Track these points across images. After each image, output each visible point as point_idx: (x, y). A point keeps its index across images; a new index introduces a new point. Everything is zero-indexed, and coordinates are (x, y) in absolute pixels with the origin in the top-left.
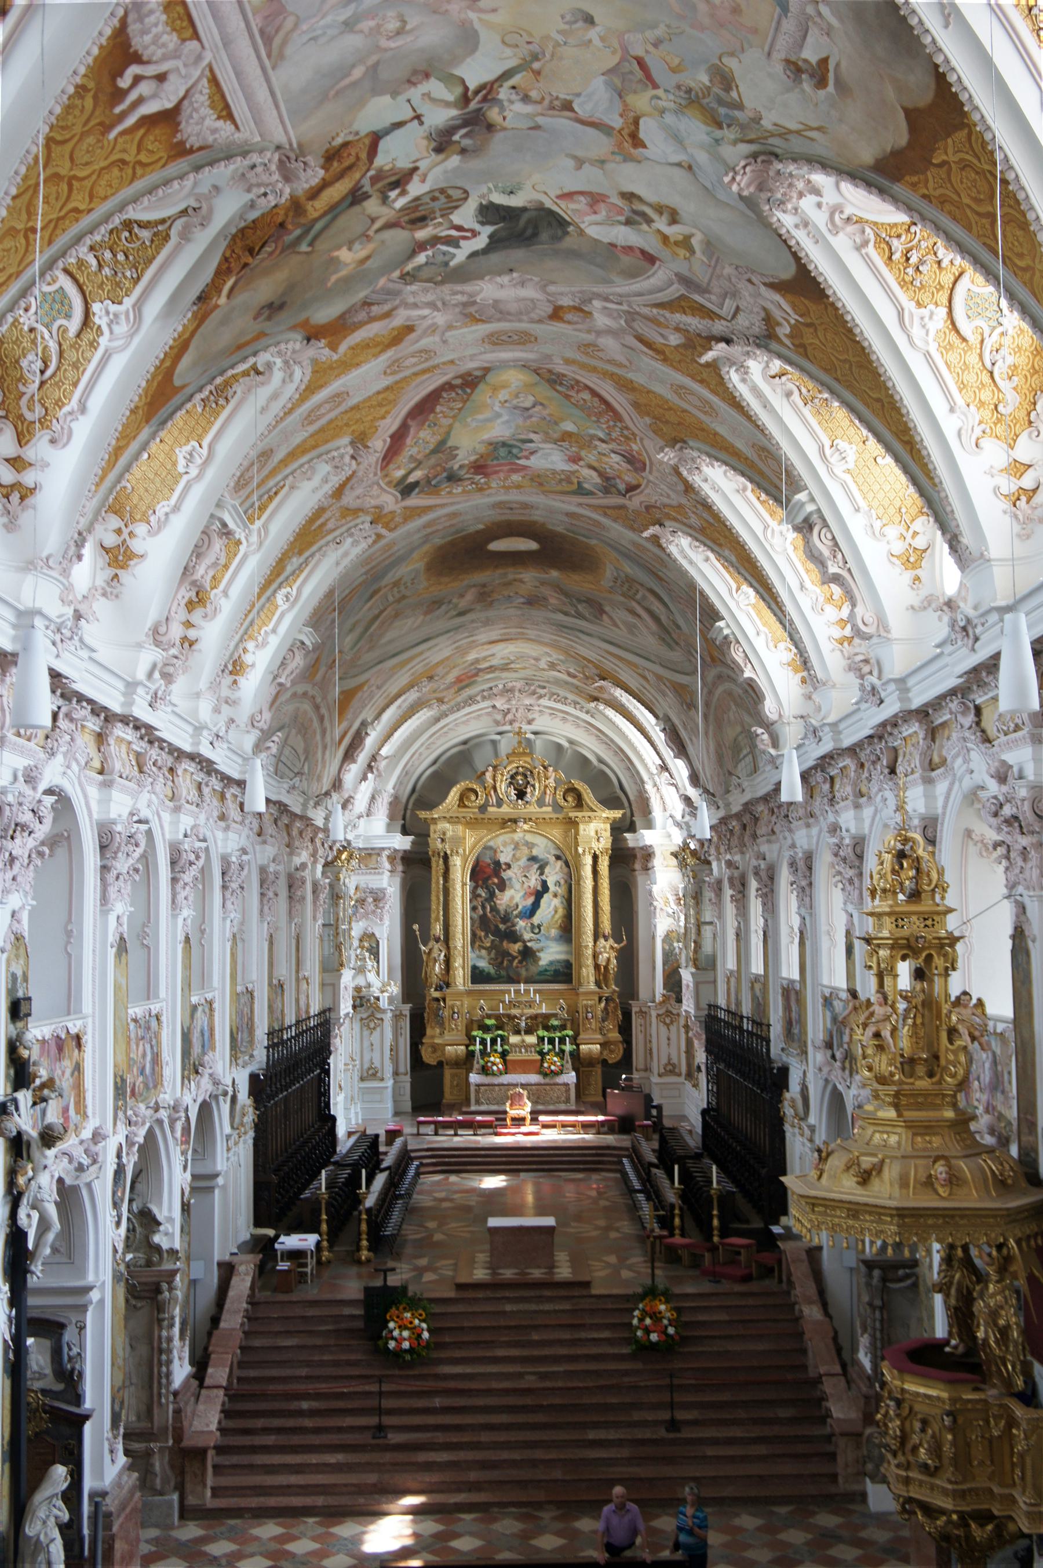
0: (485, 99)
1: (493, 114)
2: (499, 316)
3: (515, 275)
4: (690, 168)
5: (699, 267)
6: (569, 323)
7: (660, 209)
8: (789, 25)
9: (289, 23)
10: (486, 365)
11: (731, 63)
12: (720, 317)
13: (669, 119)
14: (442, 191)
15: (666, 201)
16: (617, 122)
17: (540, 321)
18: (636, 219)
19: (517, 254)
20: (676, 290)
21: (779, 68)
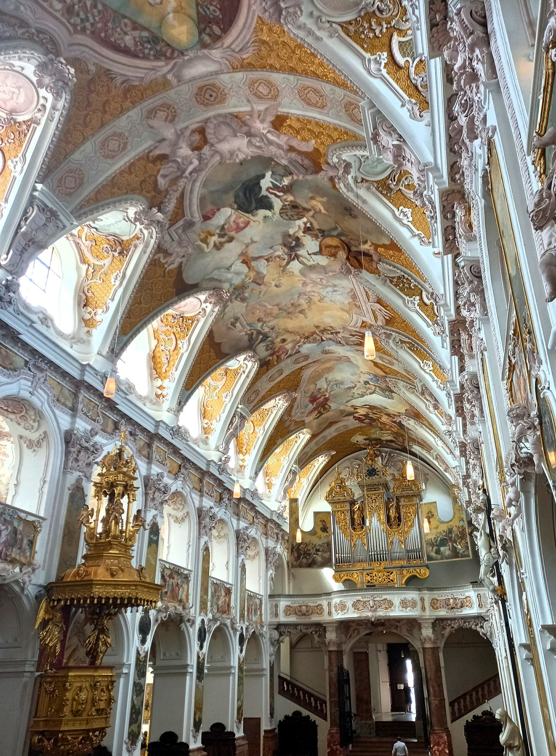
0: (291, 255)
1: (286, 250)
2: (228, 120)
3: (238, 161)
4: (228, 269)
5: (194, 235)
6: (194, 131)
7: (222, 244)
8: (245, 323)
9: (350, 294)
10: (205, 51)
11: (245, 305)
12: (171, 226)
13: (243, 277)
14: (290, 219)
15: (223, 250)
16: (253, 264)
17: (207, 121)
18: (223, 231)
19: (244, 177)
20: (188, 217)
21: (239, 315)
